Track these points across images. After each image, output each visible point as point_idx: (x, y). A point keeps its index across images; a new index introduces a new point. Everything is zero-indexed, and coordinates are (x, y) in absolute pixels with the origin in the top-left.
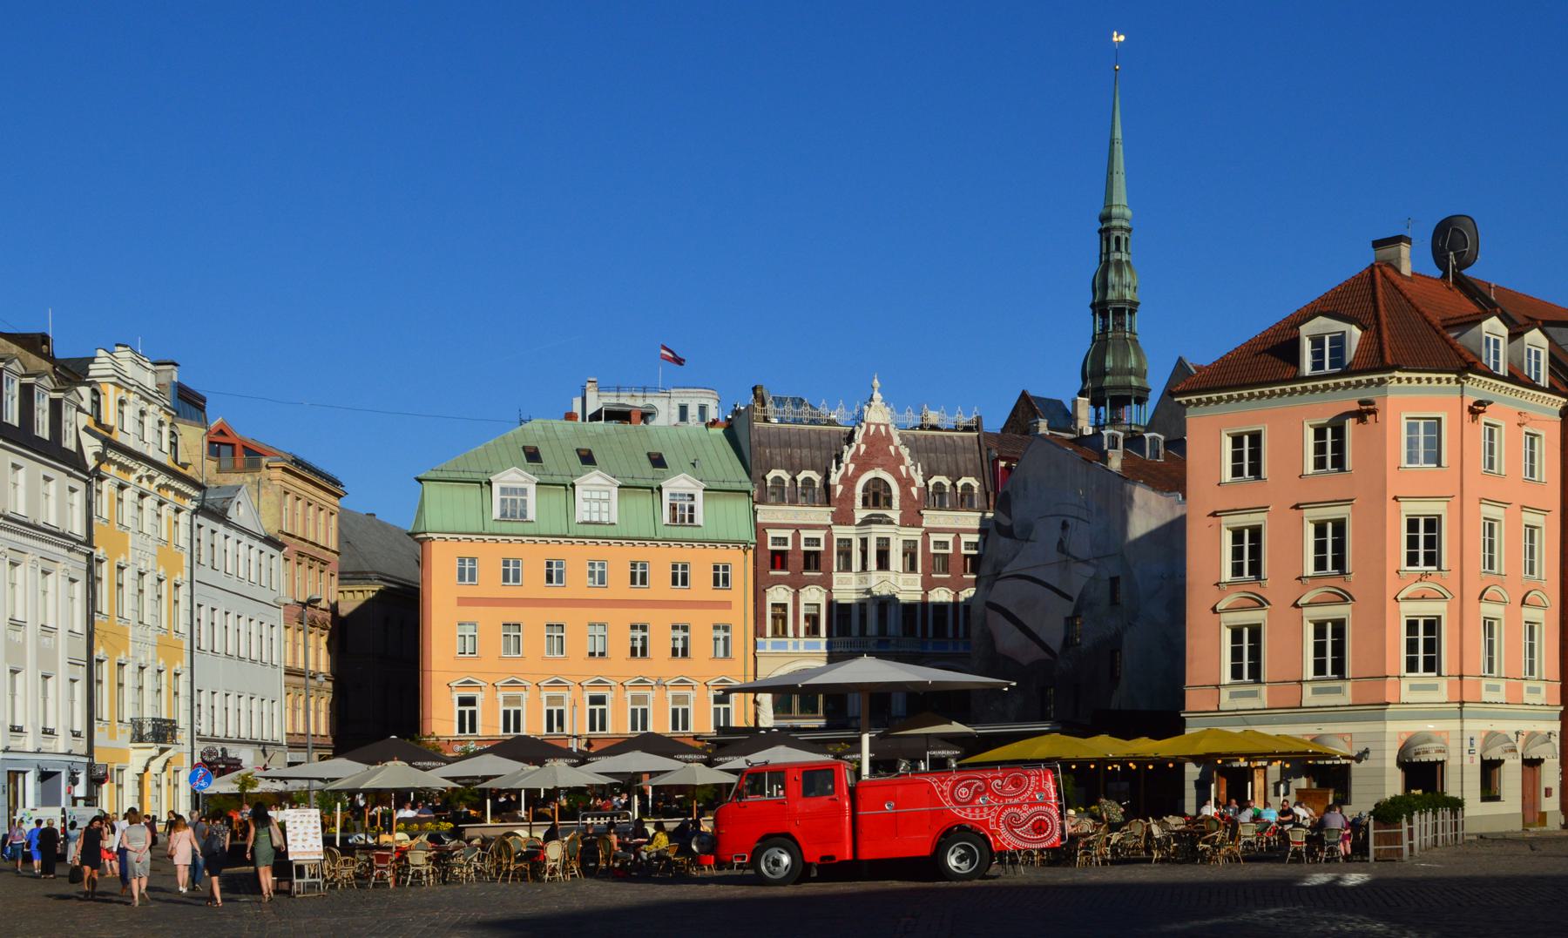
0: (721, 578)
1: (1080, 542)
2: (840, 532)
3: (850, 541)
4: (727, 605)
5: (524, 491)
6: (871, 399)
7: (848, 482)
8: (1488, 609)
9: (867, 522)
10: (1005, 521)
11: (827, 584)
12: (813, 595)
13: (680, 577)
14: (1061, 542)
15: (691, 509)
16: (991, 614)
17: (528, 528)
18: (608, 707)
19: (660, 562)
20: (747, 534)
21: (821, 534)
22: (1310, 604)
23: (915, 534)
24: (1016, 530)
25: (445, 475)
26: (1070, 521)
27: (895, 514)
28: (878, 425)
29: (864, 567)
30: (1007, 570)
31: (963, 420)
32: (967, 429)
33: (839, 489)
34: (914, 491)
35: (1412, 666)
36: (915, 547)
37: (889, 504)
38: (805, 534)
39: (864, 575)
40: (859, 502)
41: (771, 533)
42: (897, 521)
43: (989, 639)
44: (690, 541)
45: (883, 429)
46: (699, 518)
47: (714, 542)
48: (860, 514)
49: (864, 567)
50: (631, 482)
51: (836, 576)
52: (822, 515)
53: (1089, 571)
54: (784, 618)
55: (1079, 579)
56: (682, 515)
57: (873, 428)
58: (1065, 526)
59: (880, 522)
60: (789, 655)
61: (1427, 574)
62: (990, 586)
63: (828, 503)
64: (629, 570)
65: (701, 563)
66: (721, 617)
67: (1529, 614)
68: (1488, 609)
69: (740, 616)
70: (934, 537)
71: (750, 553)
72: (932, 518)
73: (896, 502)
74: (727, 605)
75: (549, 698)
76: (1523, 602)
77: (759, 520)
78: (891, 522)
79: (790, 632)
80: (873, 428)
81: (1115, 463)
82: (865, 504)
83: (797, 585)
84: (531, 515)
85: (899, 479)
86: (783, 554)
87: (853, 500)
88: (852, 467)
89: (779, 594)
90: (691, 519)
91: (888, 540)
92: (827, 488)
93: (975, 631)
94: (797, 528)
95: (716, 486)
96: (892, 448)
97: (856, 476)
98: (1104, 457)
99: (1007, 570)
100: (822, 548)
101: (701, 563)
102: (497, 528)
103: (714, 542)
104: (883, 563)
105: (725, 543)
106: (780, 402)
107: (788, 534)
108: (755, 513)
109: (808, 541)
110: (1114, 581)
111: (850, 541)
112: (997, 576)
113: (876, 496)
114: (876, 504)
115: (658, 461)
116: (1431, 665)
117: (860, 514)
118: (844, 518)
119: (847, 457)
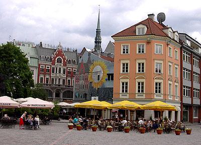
2: (52, 66)
7: (55, 58)
20: (37, 65)
35: (156, 92)
37: (61, 62)
49: (56, 72)
54: (42, 80)
67: (176, 84)
83: (45, 74)
85: (63, 58)
92: (51, 59)
104: (60, 72)
116: (160, 92)
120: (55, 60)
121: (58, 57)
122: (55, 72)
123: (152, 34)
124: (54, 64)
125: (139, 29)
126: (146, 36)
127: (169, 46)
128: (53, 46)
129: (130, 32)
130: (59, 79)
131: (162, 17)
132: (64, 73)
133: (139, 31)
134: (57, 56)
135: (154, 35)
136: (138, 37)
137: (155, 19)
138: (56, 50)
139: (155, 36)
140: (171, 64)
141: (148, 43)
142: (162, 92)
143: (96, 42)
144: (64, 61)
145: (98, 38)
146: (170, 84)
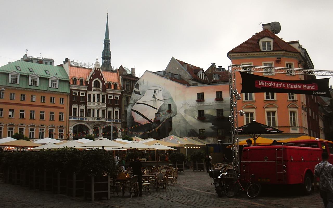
0: (62, 102)
1: (159, 95)
2: (89, 92)
4: (63, 108)
9: (94, 90)
10: (137, 90)
11: (85, 104)
12: (82, 107)
13: (52, 100)
14: (154, 96)
16: (133, 112)
18: (34, 131)
20: (68, 91)
23: (105, 94)
24: (141, 93)
26: (156, 91)
27: (101, 90)
28: (97, 68)
29: (94, 101)
30: (138, 102)
33: (89, 82)
34: (105, 84)
37: (99, 87)
39: (94, 103)
40: (93, 86)
42: (101, 91)
43: (132, 118)
45: (98, 69)
49: (94, 101)
53: (163, 103)
55: (159, 105)
57: (96, 69)
58: (155, 92)
60: (76, 121)
62: (133, 106)
64: (40, 98)
66: (61, 111)
69: (66, 112)
73: (101, 87)
74: (63, 108)
79: (77, 116)
80: (96, 69)
82: (94, 87)
83: (79, 104)
88: (92, 78)
89: (75, 106)
93: (128, 116)
94: (79, 90)
96: (100, 74)
97: (93, 79)
99: (138, 102)
100: (85, 96)
104: (98, 101)
108: (70, 86)
109: (82, 94)
110: (170, 105)
112: (135, 103)
114: (96, 87)
117: (93, 89)
120: (91, 83)
122: (92, 101)
123: (283, 50)
124: (90, 89)
125: (264, 43)
126: (275, 52)
128: (87, 64)
130: (98, 110)
132: (103, 101)
133: (264, 47)
135: (286, 51)
136: (264, 53)
138: (91, 69)
139: (286, 53)
142: (298, 124)
143: (103, 58)
145: (106, 52)
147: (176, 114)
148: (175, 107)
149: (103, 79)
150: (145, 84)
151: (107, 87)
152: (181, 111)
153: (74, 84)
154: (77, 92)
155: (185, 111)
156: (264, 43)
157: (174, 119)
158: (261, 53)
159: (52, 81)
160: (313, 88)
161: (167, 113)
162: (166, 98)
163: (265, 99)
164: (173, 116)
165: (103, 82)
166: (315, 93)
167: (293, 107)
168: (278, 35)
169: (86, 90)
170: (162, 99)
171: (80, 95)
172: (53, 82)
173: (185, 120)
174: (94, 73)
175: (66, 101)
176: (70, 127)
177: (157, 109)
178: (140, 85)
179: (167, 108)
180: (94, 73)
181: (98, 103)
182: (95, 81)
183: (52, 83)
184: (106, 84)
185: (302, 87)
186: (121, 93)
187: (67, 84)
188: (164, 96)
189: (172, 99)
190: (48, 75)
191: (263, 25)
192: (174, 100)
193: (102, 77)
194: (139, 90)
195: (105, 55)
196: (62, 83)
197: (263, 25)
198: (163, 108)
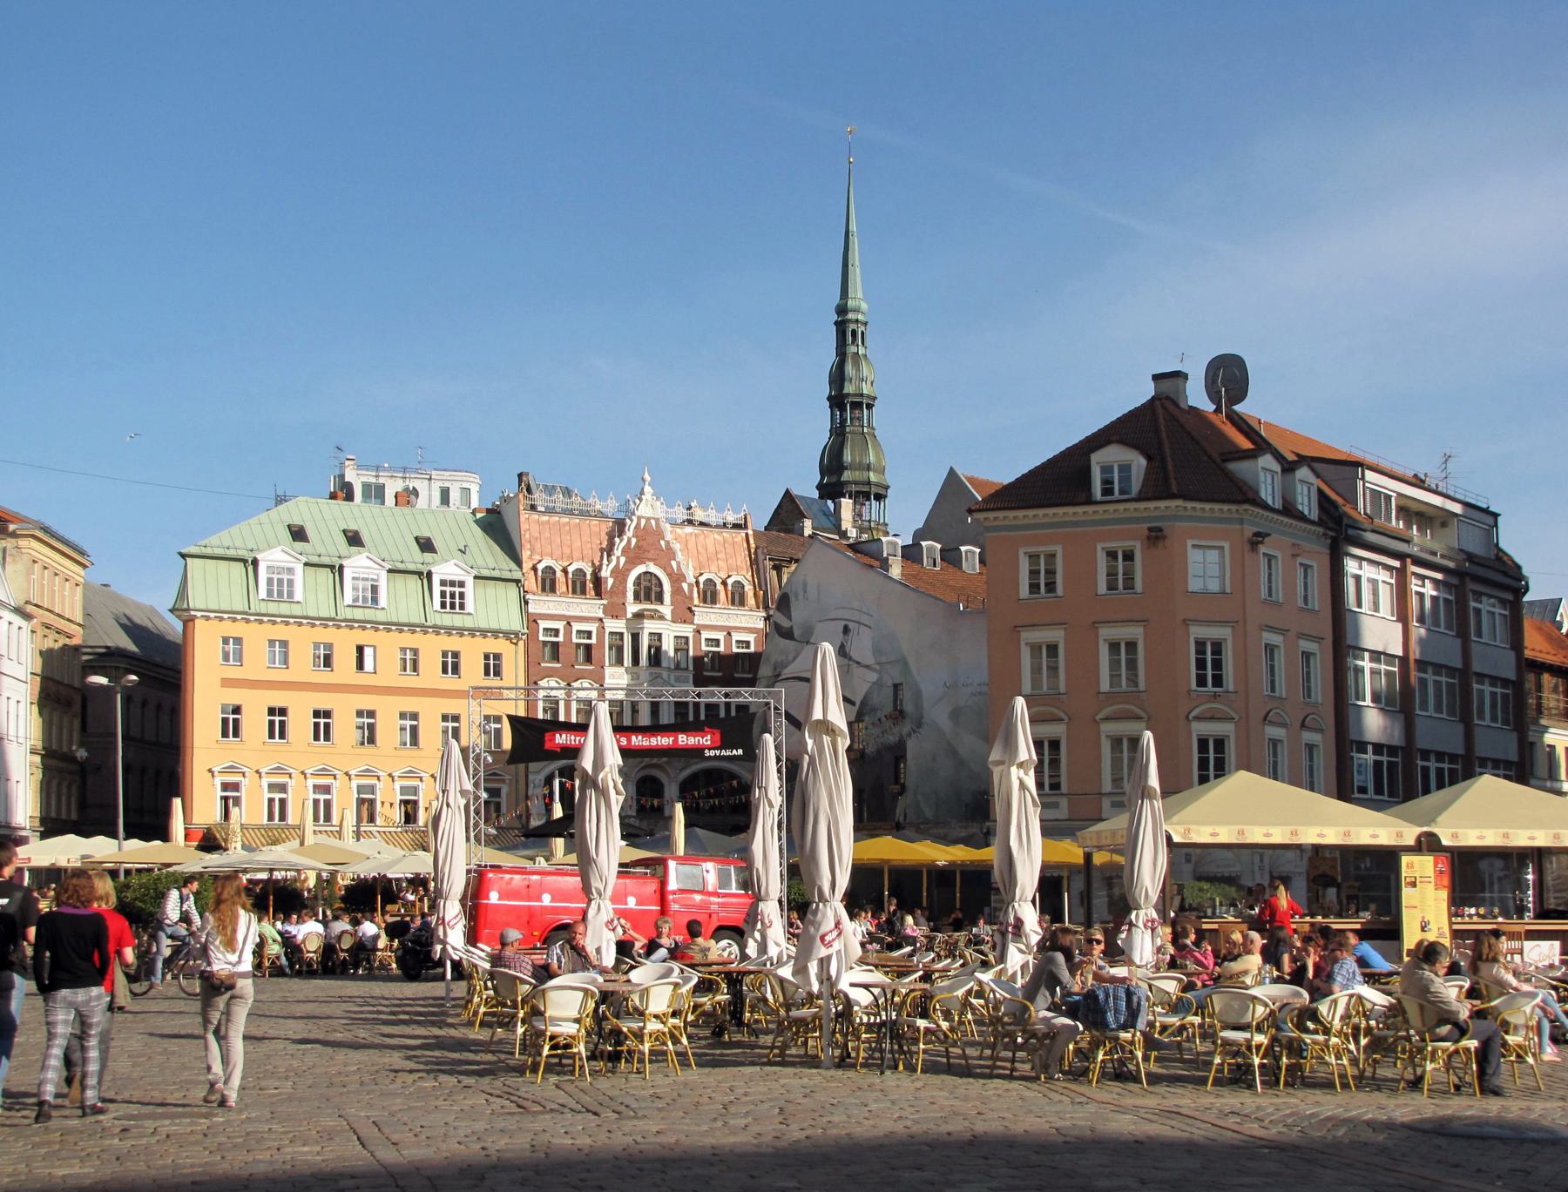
0: (493, 666)
2: (613, 625)
3: (621, 634)
5: (290, 571)
6: (642, 493)
8: (1273, 732)
9: (639, 616)
10: (785, 623)
13: (452, 664)
15: (462, 595)
17: (296, 610)
19: (431, 649)
20: (515, 623)
21: (593, 627)
22: (1107, 719)
23: (687, 630)
24: (797, 633)
25: (208, 551)
26: (851, 625)
27: (666, 609)
28: (648, 519)
30: (787, 672)
31: (731, 518)
32: (736, 526)
33: (611, 581)
34: (685, 586)
36: (687, 643)
37: (660, 599)
38: (576, 626)
41: (543, 624)
42: (669, 617)
44: (461, 631)
46: (469, 607)
47: (484, 633)
48: (632, 608)
50: (401, 566)
51: (609, 671)
52: (591, 607)
53: (873, 677)
56: (453, 600)
57: (643, 522)
58: (846, 630)
59: (652, 617)
61: (1215, 695)
63: (599, 594)
65: (473, 654)
67: (1309, 737)
68: (1273, 732)
70: (705, 635)
71: (521, 643)
72: (703, 615)
75: (315, 787)
76: (1303, 725)
77: (531, 610)
78: (662, 618)
80: (643, 522)
81: (896, 571)
82: (637, 597)
84: (298, 596)
85: (669, 575)
86: (555, 645)
87: (624, 593)
88: (623, 560)
90: (462, 606)
91: (660, 635)
92: (598, 581)
95: (486, 573)
98: (885, 564)
99: (787, 672)
101: (473, 654)
102: (263, 608)
103: (484, 633)
105: (496, 633)
106: (550, 490)
107: (560, 625)
108: (526, 603)
110: (896, 687)
111: (621, 634)
113: (648, 591)
114: (648, 599)
115: (426, 545)
118: (615, 611)
119: (618, 552)
121: (640, 569)
127: (1262, 549)
129: (1061, 480)
131: (1229, 376)
134: (634, 560)
137: (1197, 396)
140: (1275, 639)
141: (1156, 536)
143: (837, 401)
144: (677, 591)
146: (1274, 743)
147: (919, 724)
148: (918, 695)
149: (674, 563)
150: (812, 591)
151: (696, 602)
152: (939, 715)
153: (544, 590)
154: (560, 625)
155: (955, 715)
156: (1106, 469)
157: (912, 746)
158: (1090, 509)
159: (443, 583)
160: (706, 740)
161: (888, 724)
162: (884, 659)
163: (1105, 686)
164: (909, 735)
165: (677, 578)
166: (712, 753)
167: (1212, 718)
168: (1237, 408)
169: (601, 615)
170: (870, 660)
171: (575, 640)
172: (448, 589)
173: (952, 752)
174: (634, 541)
175: (514, 661)
176: (531, 777)
177: (853, 704)
178: (792, 599)
179: (884, 700)
180: (634, 541)
181: (656, 670)
182: (639, 577)
183: (443, 594)
184: (690, 585)
185: (676, 741)
186: (761, 625)
187: (513, 591)
188: (877, 651)
189: (905, 663)
190: (428, 556)
191: (1156, 378)
192: (913, 667)
193: (671, 554)
194: (790, 618)
195: (842, 387)
196: (492, 589)
197: (1156, 378)
198: (876, 700)
